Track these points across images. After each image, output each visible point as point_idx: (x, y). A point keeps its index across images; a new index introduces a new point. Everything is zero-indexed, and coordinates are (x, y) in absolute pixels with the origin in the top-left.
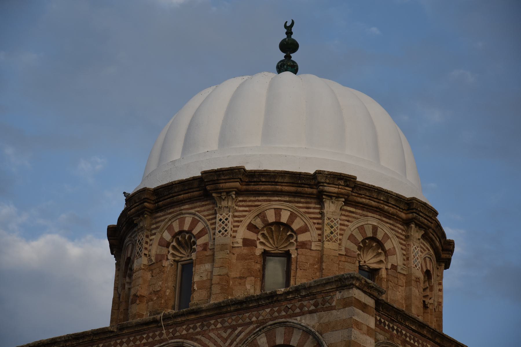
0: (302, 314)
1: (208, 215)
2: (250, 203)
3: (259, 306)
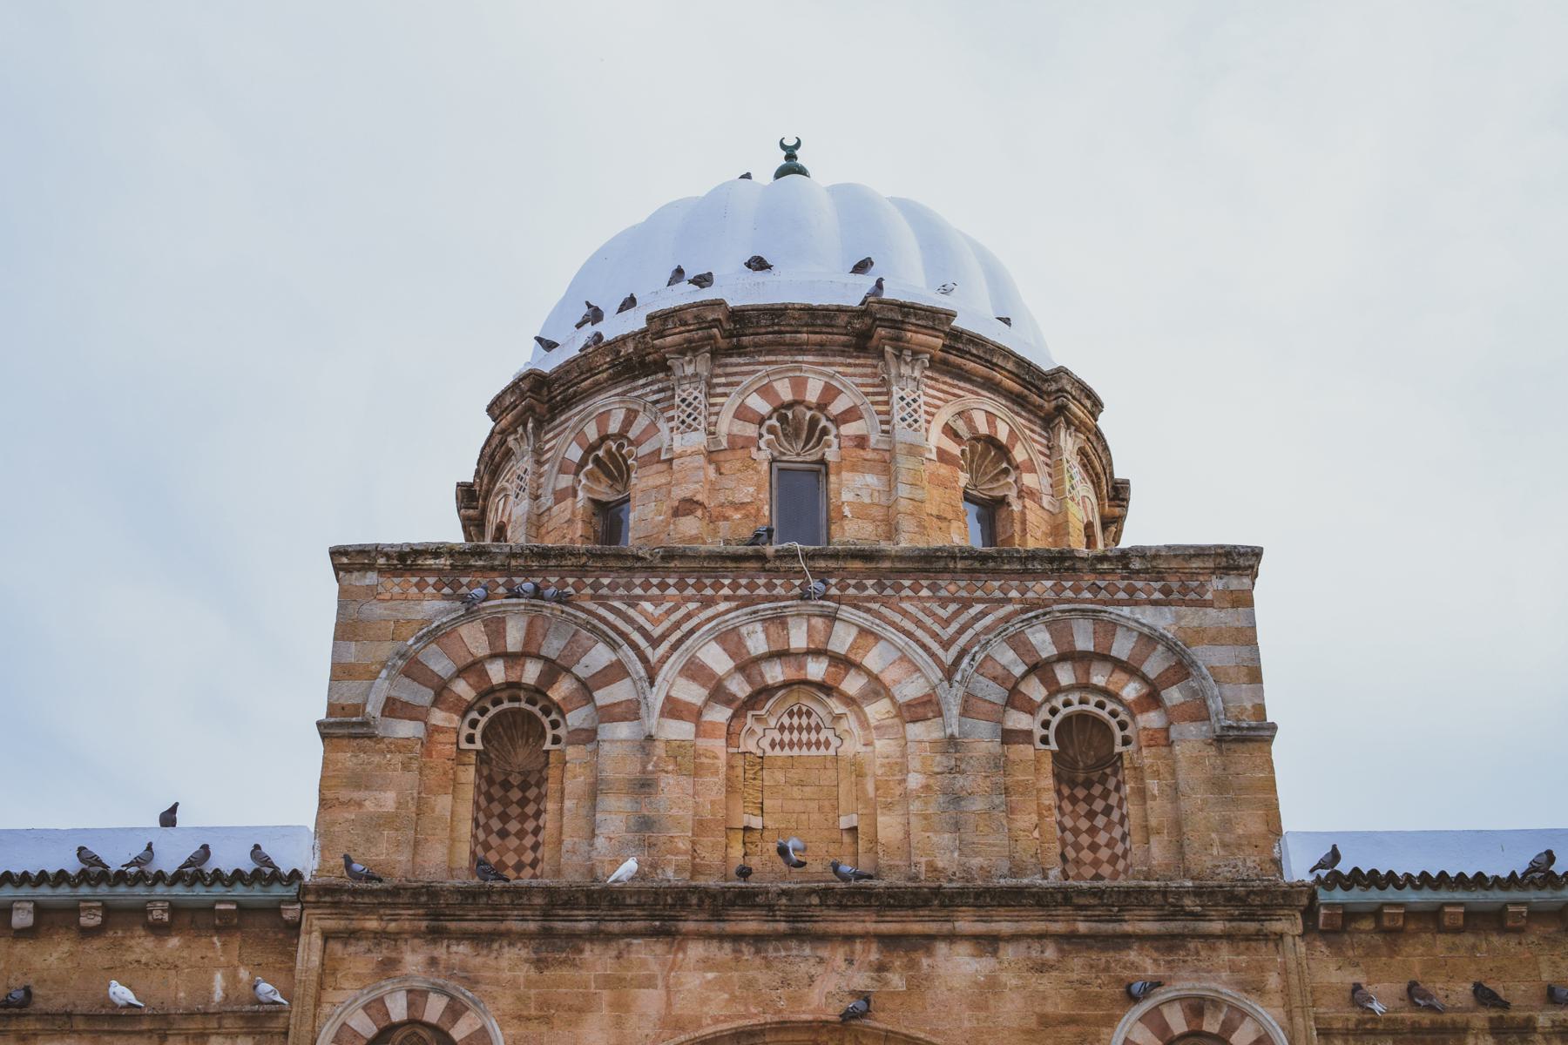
0: (1137, 603)
1: (863, 385)
2: (945, 387)
3: (1026, 571)
